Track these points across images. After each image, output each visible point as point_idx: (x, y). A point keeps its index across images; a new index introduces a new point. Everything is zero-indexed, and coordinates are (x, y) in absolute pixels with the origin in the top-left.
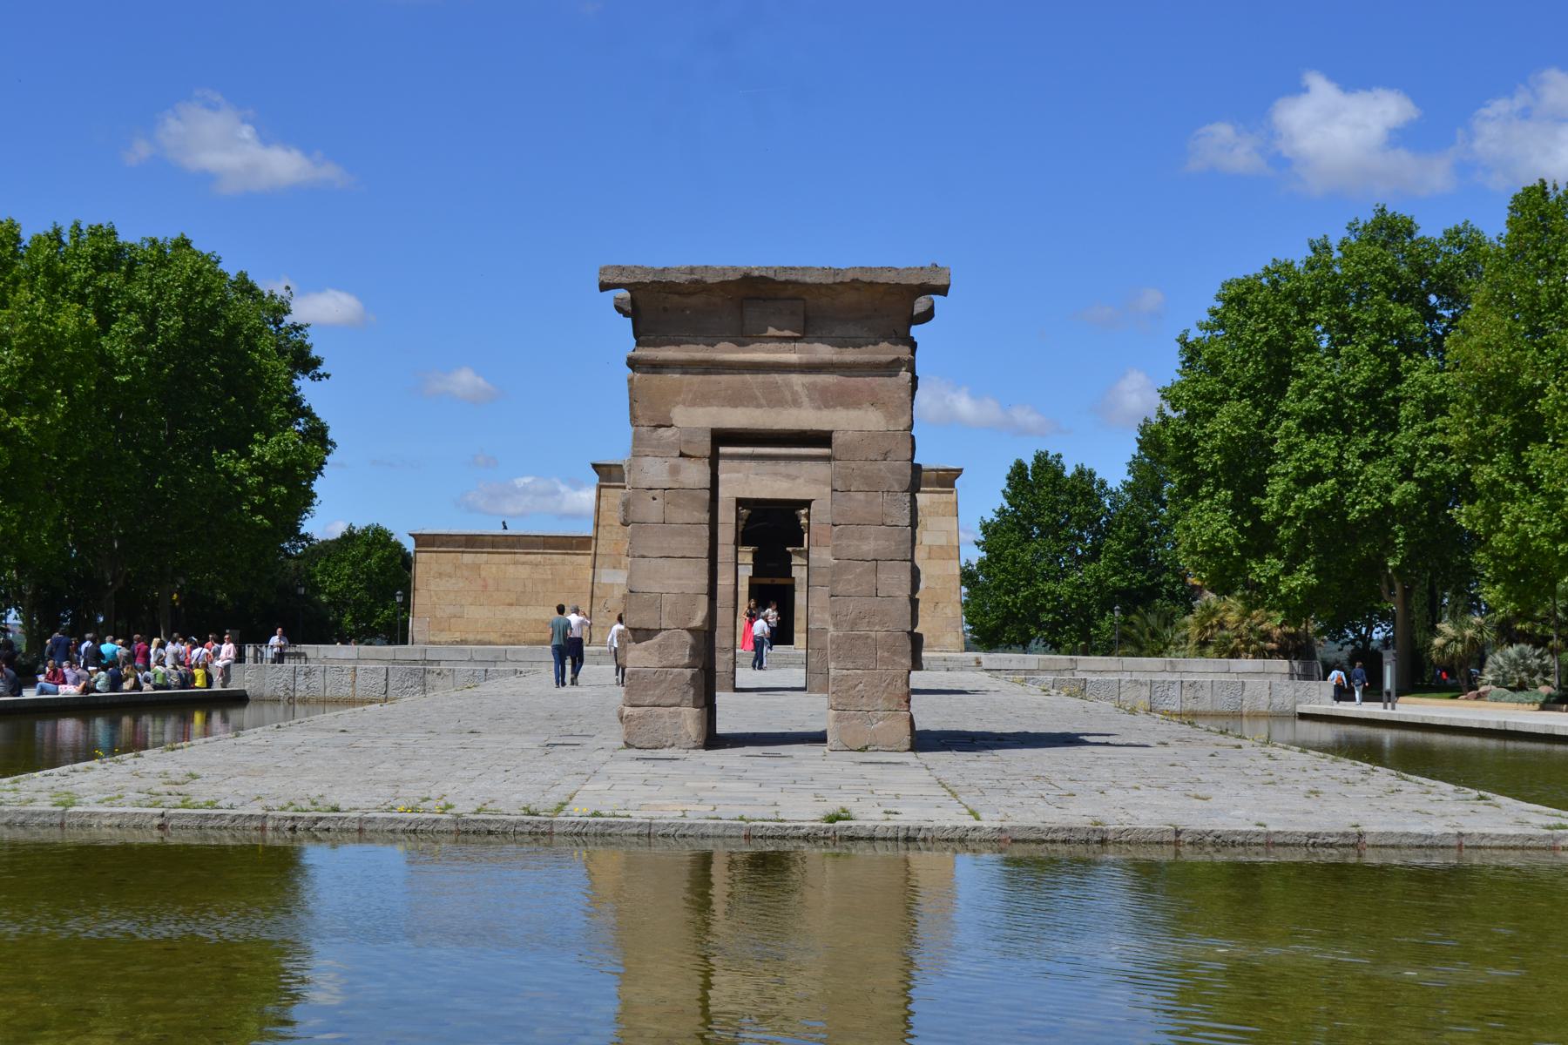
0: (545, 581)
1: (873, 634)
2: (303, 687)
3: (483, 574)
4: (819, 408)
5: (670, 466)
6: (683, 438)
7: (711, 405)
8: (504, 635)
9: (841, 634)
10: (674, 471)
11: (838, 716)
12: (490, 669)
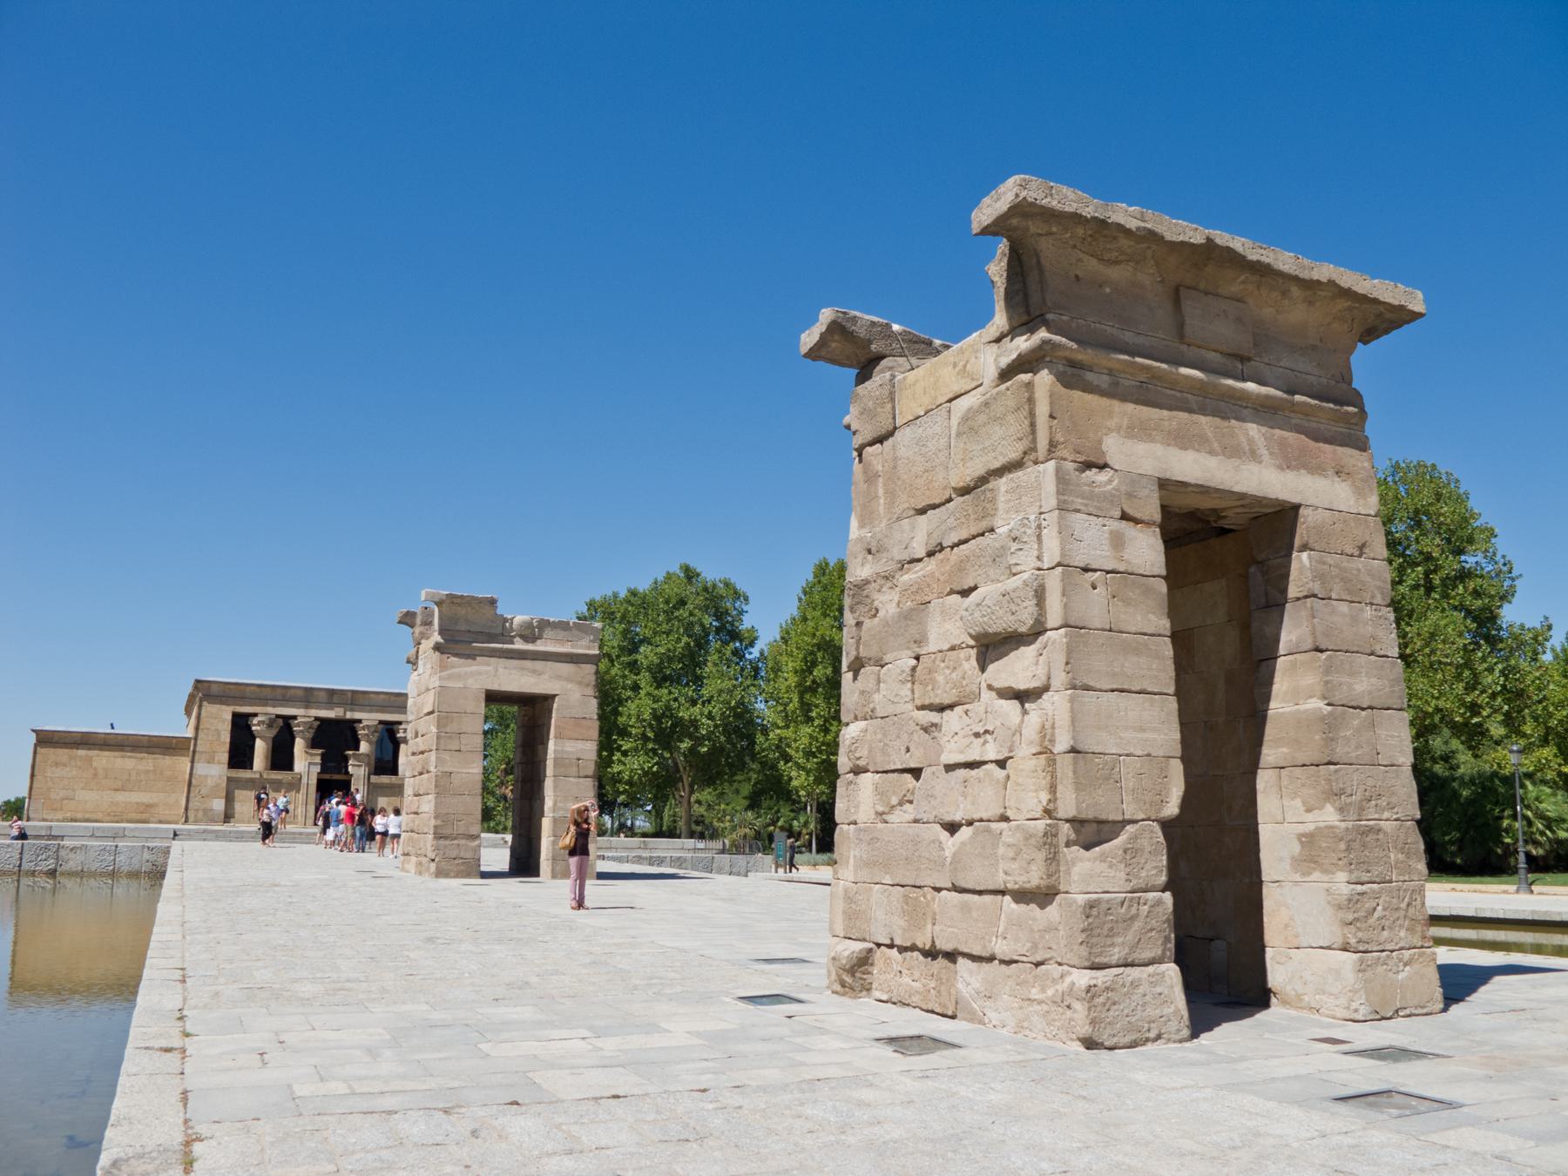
0: (147, 772)
3: (95, 764)
5: (1111, 532)
7: (1153, 441)
8: (109, 815)
10: (1117, 542)
11: (1362, 961)
12: (120, 844)
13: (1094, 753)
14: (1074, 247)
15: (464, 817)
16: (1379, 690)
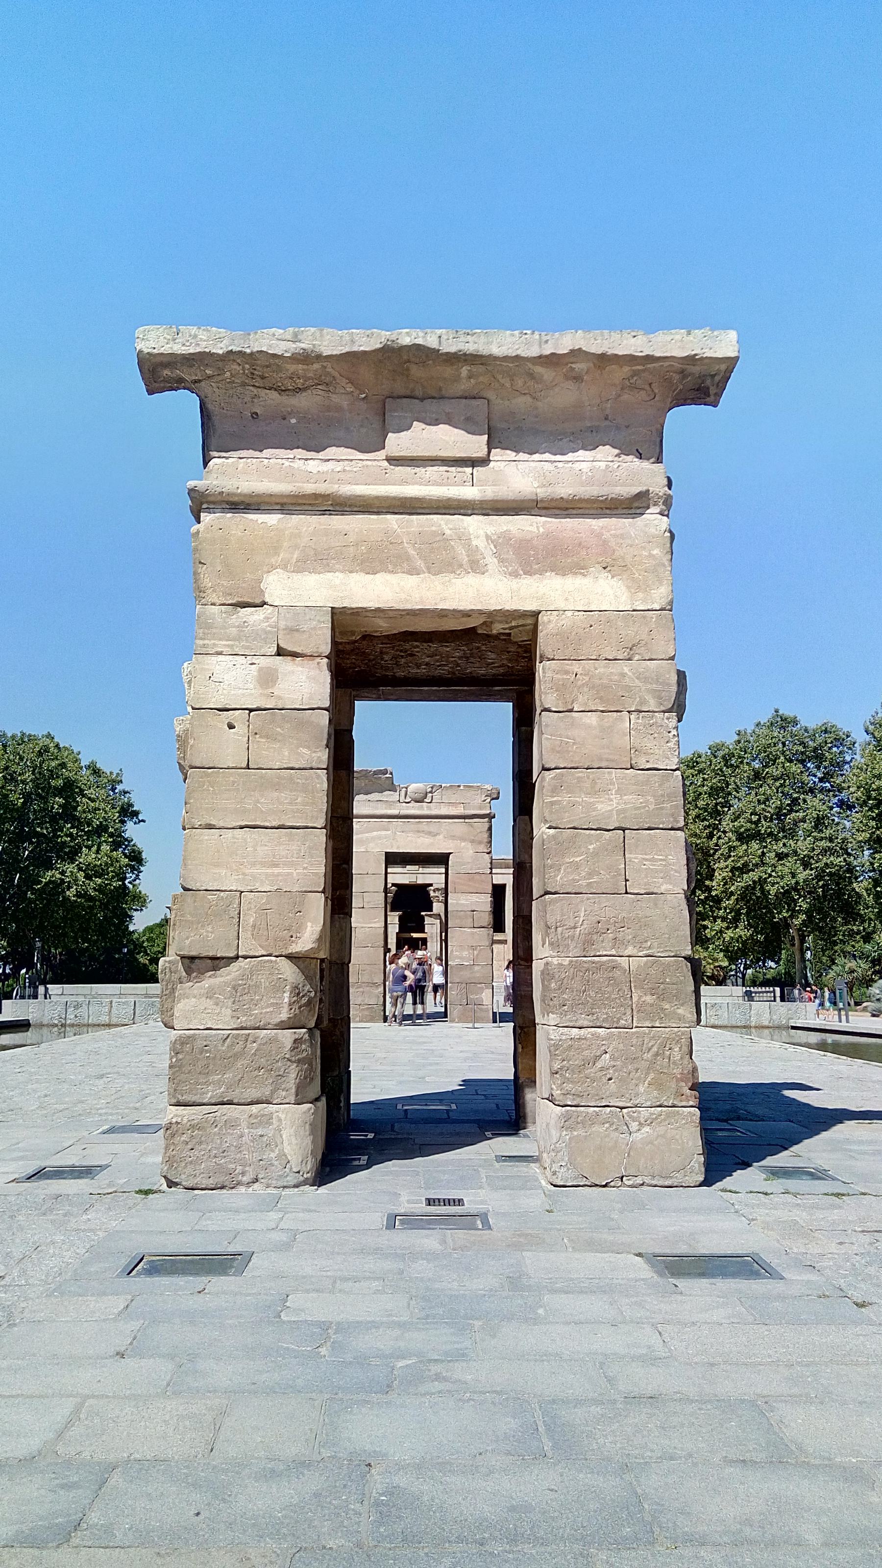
1: (623, 961)
2: (72, 1016)
4: (515, 575)
6: (282, 624)
9: (566, 961)
10: (267, 679)
11: (567, 1118)
13: (206, 890)
14: (244, 384)
15: (367, 967)
16: (639, 808)
